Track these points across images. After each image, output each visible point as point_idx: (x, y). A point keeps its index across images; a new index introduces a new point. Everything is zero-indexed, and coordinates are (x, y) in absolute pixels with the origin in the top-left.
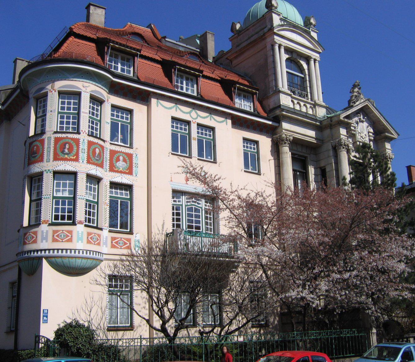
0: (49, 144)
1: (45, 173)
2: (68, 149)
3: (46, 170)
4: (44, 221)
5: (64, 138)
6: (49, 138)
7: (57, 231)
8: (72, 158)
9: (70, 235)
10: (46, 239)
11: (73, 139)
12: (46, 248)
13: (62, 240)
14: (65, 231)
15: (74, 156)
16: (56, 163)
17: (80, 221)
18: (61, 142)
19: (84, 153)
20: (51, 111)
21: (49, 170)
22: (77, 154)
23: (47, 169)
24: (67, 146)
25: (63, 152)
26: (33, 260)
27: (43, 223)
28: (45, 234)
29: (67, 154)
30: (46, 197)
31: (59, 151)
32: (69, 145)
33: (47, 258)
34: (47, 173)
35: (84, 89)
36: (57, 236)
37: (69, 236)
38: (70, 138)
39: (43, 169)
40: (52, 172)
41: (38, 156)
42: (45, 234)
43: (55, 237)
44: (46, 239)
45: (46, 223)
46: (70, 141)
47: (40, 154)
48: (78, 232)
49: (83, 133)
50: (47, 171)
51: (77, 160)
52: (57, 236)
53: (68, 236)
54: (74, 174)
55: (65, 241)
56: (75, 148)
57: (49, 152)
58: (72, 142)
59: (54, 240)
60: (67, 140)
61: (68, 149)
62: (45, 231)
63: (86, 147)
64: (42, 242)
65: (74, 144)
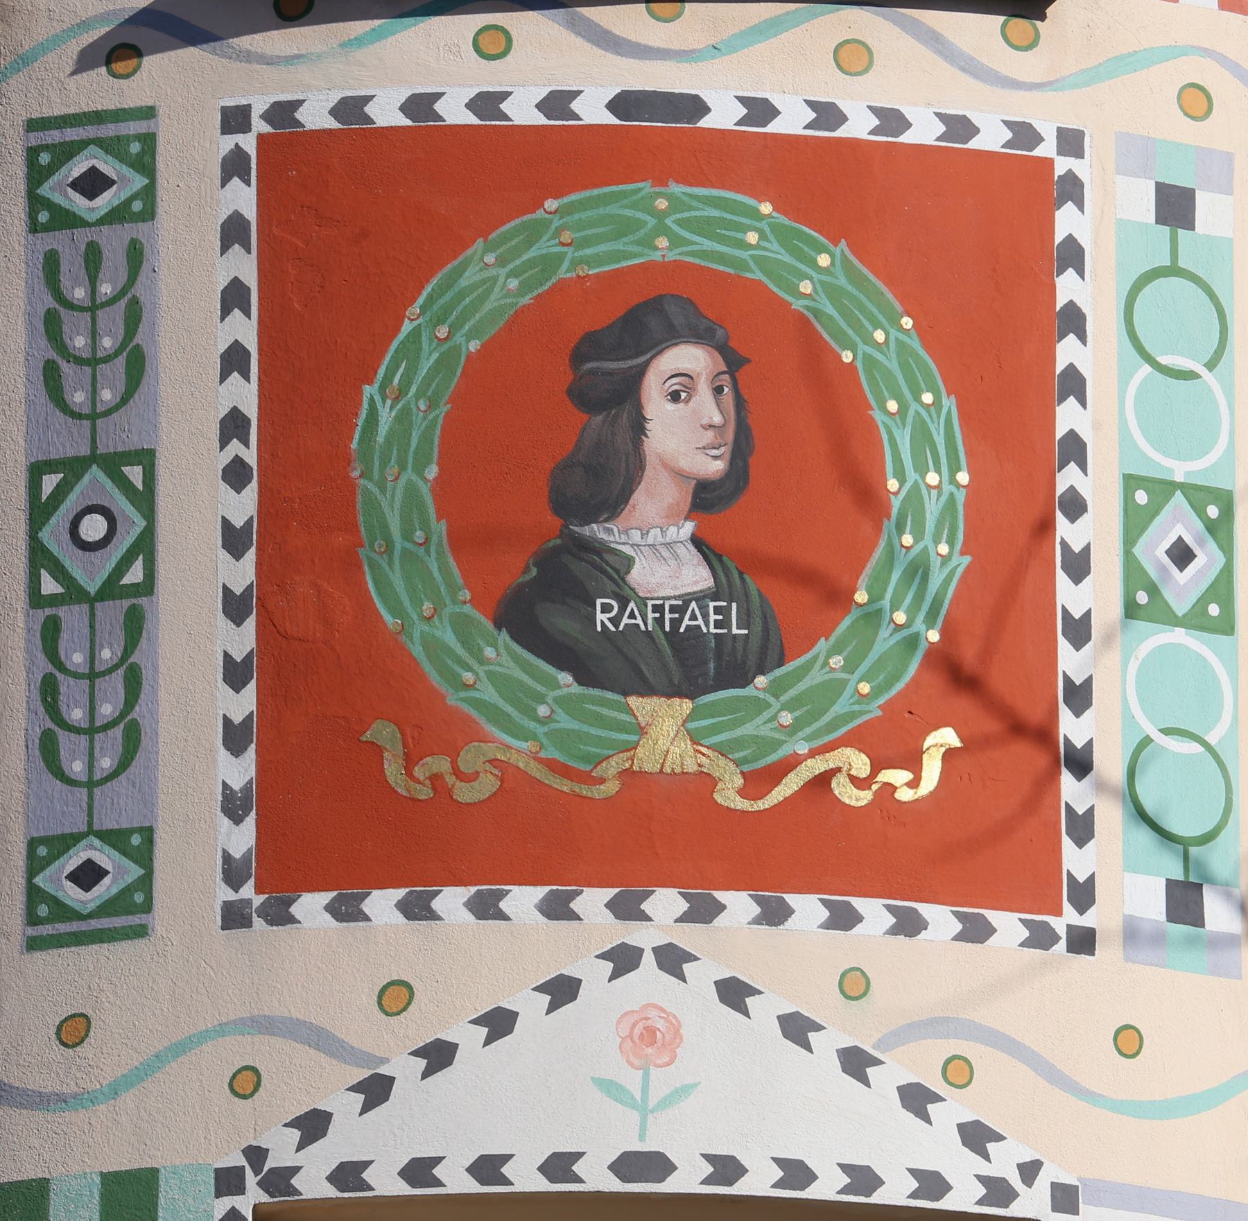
2: (705, 498)
5: (554, 158)
8: (853, 777)
11: (827, 179)
15: (893, 744)
16: (335, 952)
24: (682, 426)
29: (693, 665)
32: (733, 362)
58: (816, 275)
60: (666, 227)
65: (882, 343)
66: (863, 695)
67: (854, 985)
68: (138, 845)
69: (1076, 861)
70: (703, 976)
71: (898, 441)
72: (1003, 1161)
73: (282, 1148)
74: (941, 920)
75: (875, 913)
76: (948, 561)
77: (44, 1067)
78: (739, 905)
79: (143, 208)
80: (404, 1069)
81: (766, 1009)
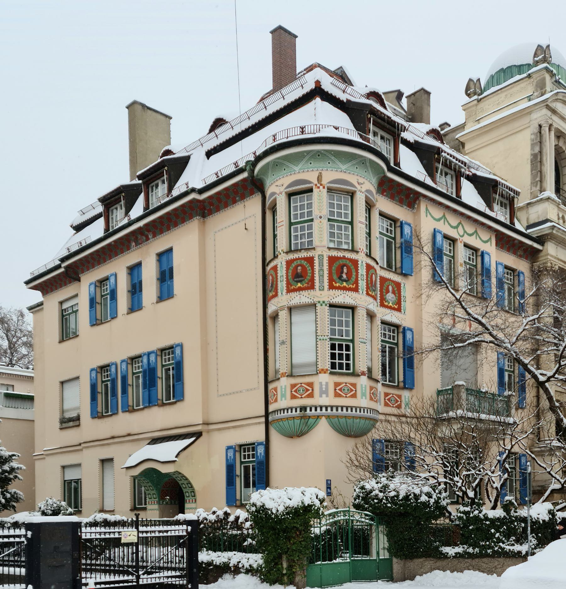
0: (321, 264)
1: (318, 305)
3: (319, 302)
4: (322, 370)
6: (321, 257)
7: (339, 384)
8: (351, 286)
11: (351, 260)
12: (327, 404)
13: (346, 395)
15: (353, 285)
16: (333, 292)
17: (363, 372)
20: (321, 217)
21: (324, 302)
24: (345, 270)
26: (309, 419)
27: (320, 373)
28: (324, 387)
30: (322, 338)
31: (335, 277)
33: (328, 417)
34: (321, 305)
36: (340, 390)
38: (348, 259)
39: (316, 300)
41: (306, 281)
42: (324, 387)
43: (337, 391)
45: (325, 373)
47: (308, 278)
50: (321, 302)
51: (356, 290)
52: (340, 390)
53: (352, 390)
54: (353, 309)
56: (354, 274)
57: (321, 276)
58: (350, 264)
59: (337, 395)
60: (344, 262)
61: (346, 274)
62: (324, 383)
64: (321, 396)
65: (352, 267)
66: (352, 283)
77: (319, 296)
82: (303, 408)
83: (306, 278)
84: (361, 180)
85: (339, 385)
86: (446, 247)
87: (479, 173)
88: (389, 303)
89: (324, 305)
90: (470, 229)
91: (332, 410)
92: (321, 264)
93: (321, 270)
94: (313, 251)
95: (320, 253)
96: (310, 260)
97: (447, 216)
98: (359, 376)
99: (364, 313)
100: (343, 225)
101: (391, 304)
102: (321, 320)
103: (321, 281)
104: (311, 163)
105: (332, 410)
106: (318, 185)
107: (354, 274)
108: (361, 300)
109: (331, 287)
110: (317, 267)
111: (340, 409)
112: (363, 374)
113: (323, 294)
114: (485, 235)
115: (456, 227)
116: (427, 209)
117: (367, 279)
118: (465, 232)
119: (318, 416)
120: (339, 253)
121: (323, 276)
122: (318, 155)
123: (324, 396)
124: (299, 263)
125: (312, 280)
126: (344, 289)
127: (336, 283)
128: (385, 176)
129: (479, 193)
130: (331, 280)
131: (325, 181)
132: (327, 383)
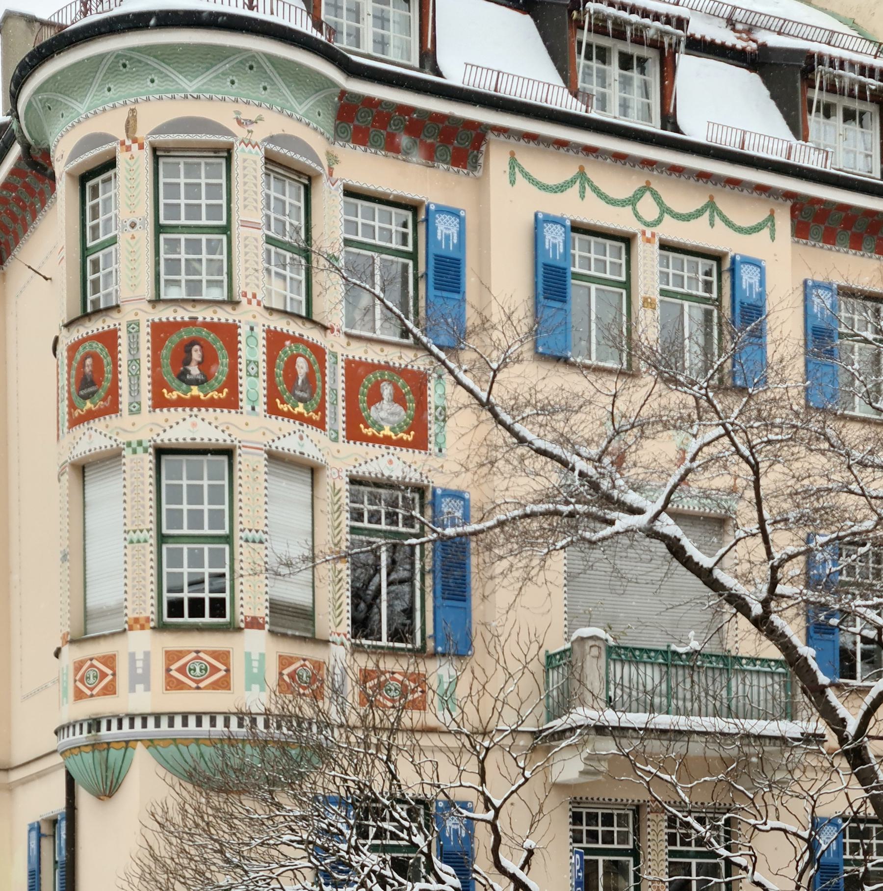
0: (134, 347)
1: (127, 452)
2: (199, 364)
3: (129, 444)
4: (136, 620)
8: (215, 395)
9: (223, 667)
10: (145, 679)
11: (212, 327)
12: (148, 710)
13: (197, 682)
14: (205, 652)
15: (220, 391)
17: (254, 619)
18: (175, 339)
19: (257, 376)
21: (140, 443)
22: (232, 382)
23: (134, 439)
25: (183, 376)
26: (108, 750)
27: (131, 629)
29: (197, 382)
31: (169, 377)
32: (202, 347)
33: (151, 743)
34: (134, 452)
35: (241, 133)
36: (182, 670)
37: (219, 670)
39: (122, 439)
40: (151, 450)
42: (139, 664)
44: (145, 679)
45: (142, 628)
46: (204, 332)
47: (106, 384)
48: (248, 655)
49: (250, 302)
50: (134, 445)
51: (231, 403)
52: (182, 670)
53: (215, 670)
55: (206, 688)
57: (135, 376)
58: (211, 337)
59: (173, 684)
60: (193, 332)
61: (199, 364)
62: (140, 656)
63: (260, 354)
64: (132, 689)
67: (216, 419)
68: (139, 404)
69: (241, 404)
70: (200, 417)
71: (220, 356)
72: (233, 438)
73: (155, 437)
74: (226, 411)
75: (218, 410)
76: (226, 369)
78: (203, 409)
79: (138, 331)
80: (168, 428)
81: (206, 421)
82: (95, 724)
83: (100, 385)
84: (250, 113)
85: (179, 659)
86: (587, 258)
87: (773, 40)
88: (381, 428)
89: (140, 450)
90: (683, 199)
91: (158, 725)
92: (134, 347)
93: (135, 361)
94: (114, 314)
95: (132, 317)
96: (110, 339)
97: (590, 173)
98: (240, 629)
99: (261, 460)
100: (204, 238)
101: (387, 431)
102: (132, 491)
103: (135, 390)
104: (109, 90)
105: (158, 725)
106: (128, 143)
107: (224, 360)
108: (250, 427)
109: (159, 402)
110: (124, 355)
111: (178, 720)
112: (254, 623)
113: (141, 424)
114: (746, 213)
115: (632, 201)
116: (513, 163)
117: (271, 374)
118: (665, 210)
119: (127, 742)
120: (180, 310)
121: (138, 376)
122: (123, 63)
123: (140, 687)
124: (88, 349)
125: (114, 391)
126: (195, 403)
127: (170, 391)
128: (343, 93)
129: (773, 97)
130: (158, 384)
131: (143, 131)
132: (147, 654)
